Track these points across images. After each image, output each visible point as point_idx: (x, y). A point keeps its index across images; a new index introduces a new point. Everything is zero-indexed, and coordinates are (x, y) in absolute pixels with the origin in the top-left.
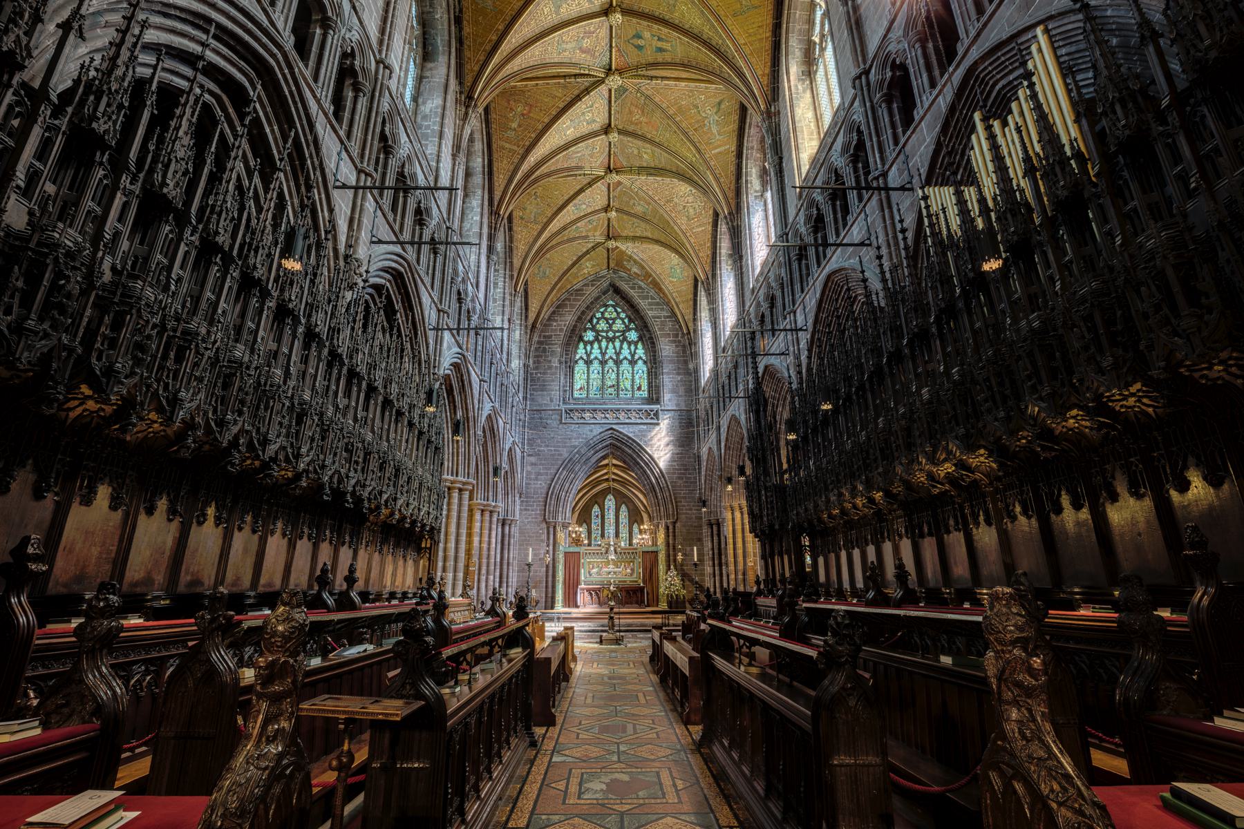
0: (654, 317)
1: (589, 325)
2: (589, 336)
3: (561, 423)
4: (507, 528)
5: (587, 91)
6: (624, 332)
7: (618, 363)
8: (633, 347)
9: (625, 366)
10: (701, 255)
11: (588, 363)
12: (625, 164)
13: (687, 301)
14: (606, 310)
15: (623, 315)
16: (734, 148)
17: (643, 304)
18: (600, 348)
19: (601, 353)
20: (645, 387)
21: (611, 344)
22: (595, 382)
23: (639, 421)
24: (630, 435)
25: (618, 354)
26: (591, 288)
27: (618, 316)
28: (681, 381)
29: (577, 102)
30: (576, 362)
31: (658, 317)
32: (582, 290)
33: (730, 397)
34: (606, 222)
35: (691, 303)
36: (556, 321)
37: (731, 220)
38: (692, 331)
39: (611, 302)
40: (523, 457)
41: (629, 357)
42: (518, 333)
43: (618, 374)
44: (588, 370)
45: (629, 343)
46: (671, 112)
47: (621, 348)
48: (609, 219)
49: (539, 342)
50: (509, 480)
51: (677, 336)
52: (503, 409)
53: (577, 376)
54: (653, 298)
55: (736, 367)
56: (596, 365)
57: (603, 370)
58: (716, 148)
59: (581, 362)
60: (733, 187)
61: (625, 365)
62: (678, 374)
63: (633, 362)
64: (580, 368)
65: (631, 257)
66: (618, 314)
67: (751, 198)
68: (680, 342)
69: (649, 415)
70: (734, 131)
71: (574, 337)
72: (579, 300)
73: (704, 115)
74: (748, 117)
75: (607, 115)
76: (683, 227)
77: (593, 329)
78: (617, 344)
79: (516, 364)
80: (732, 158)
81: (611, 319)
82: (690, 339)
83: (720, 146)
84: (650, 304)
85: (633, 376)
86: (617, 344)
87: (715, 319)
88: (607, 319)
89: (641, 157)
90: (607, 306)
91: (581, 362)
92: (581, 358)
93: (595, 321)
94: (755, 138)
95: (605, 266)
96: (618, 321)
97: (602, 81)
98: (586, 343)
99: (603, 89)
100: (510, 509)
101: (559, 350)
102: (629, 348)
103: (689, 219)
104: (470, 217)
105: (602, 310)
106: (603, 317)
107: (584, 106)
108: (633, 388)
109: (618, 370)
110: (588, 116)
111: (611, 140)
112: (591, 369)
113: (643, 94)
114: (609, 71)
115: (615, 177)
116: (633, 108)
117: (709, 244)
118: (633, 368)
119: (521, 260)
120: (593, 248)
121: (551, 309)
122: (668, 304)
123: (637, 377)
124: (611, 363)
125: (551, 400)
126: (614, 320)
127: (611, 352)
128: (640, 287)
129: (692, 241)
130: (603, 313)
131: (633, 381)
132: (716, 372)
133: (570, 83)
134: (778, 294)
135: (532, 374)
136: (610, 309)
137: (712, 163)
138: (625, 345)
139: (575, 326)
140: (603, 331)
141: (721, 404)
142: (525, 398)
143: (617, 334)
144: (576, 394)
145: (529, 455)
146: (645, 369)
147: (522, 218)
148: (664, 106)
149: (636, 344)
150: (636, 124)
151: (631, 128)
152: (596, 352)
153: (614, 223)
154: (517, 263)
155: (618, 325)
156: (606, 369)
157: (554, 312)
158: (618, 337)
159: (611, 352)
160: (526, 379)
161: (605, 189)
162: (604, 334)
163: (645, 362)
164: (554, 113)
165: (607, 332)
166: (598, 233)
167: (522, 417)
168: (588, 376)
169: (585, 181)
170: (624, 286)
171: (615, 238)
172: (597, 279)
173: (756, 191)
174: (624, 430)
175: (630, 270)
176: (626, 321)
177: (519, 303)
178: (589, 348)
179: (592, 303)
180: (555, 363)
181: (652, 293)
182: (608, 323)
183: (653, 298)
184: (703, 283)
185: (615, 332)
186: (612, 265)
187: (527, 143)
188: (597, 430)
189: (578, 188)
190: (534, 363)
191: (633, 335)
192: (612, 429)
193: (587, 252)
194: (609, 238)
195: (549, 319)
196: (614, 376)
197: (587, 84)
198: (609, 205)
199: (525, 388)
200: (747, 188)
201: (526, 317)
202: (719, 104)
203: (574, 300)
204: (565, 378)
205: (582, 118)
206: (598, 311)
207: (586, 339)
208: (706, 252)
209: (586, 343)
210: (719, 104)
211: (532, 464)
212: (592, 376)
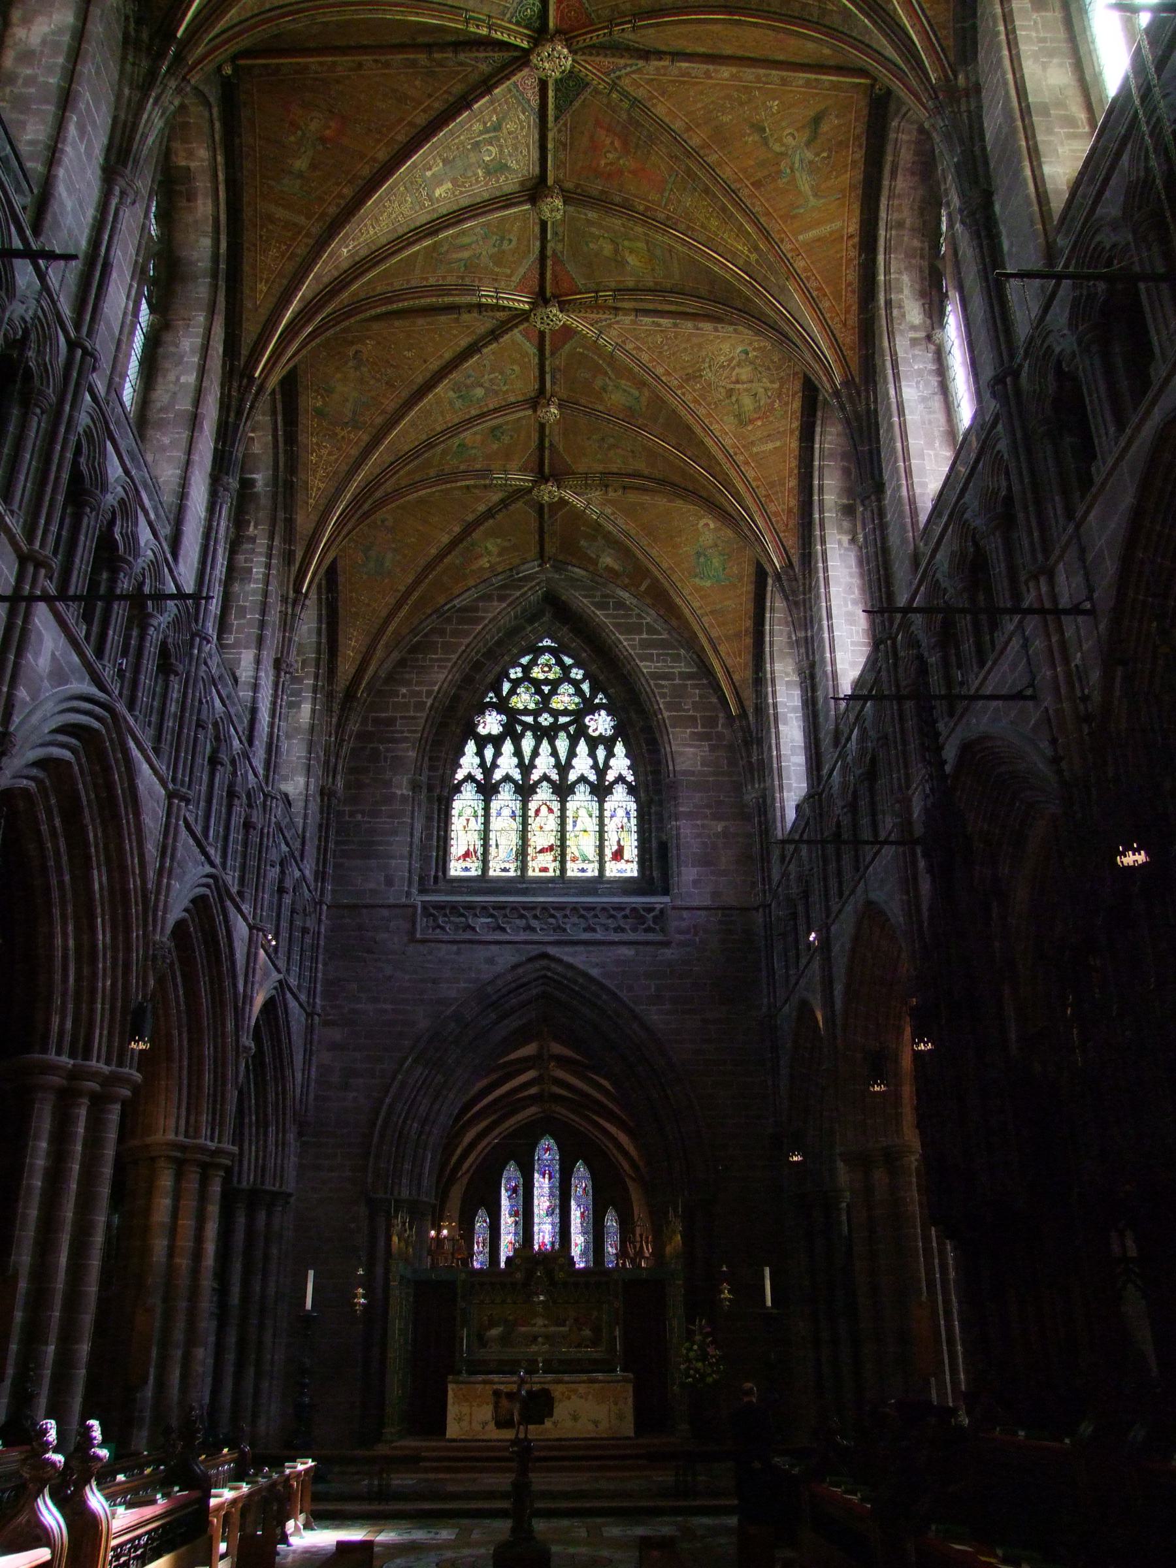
0: (656, 676)
1: (491, 697)
3: (413, 940)
4: (262, 1217)
5: (486, 86)
6: (578, 716)
7: (563, 790)
8: (601, 753)
9: (581, 800)
10: (772, 508)
11: (488, 790)
12: (581, 282)
13: (738, 635)
14: (533, 662)
15: (577, 674)
16: (853, 227)
17: (627, 644)
18: (518, 753)
19: (521, 765)
21: (545, 743)
23: (616, 937)
24: (594, 972)
25: (563, 768)
26: (498, 607)
27: (566, 678)
28: (725, 834)
29: (459, 113)
30: (457, 789)
31: (665, 676)
32: (476, 609)
33: (951, 699)
34: (535, 436)
35: (749, 641)
36: (408, 683)
37: (850, 397)
38: (750, 711)
39: (547, 642)
40: (310, 1029)
41: (592, 777)
42: (306, 708)
43: (563, 818)
44: (487, 809)
45: (593, 743)
46: (695, 141)
47: (572, 754)
48: (542, 427)
49: (362, 736)
50: (271, 1089)
51: (711, 722)
52: (249, 893)
53: (457, 824)
54: (651, 630)
55: (871, 776)
56: (506, 799)
57: (525, 808)
58: (810, 227)
59: (469, 791)
60: (853, 320)
61: (581, 800)
62: (717, 817)
63: (601, 791)
64: (466, 803)
65: (597, 527)
66: (566, 669)
67: (902, 344)
68: (720, 736)
69: (642, 920)
70: (852, 187)
72: (466, 634)
73: (777, 148)
74: (889, 148)
75: (535, 154)
76: (728, 442)
77: (502, 706)
79: (295, 785)
80: (849, 251)
81: (547, 682)
82: (747, 730)
83: (818, 223)
84: (645, 644)
85: (601, 824)
86: (562, 744)
87: (812, 666)
88: (537, 683)
89: (622, 263)
90: (538, 652)
91: (469, 791)
92: (470, 778)
93: (506, 687)
94: (906, 202)
95: (534, 551)
96: (566, 688)
97: (522, 59)
99: (525, 80)
100: (271, 1164)
101: (412, 754)
102: (592, 754)
103: (742, 421)
104: (171, 377)
105: (525, 660)
106: (527, 677)
107: (478, 127)
108: (601, 854)
109: (563, 809)
110: (490, 154)
111: (547, 214)
112: (495, 805)
113: (625, 94)
114: (540, 33)
115: (557, 317)
116: (601, 134)
117: (793, 483)
118: (601, 802)
119: (314, 517)
120: (505, 503)
121: (396, 656)
122: (690, 642)
123: (611, 826)
124: (544, 793)
125: (389, 882)
127: (544, 764)
128: (620, 605)
129: (751, 474)
131: (601, 833)
132: (815, 798)
133: (440, 64)
134: (994, 545)
135: (340, 814)
136: (546, 658)
137: (800, 264)
138: (582, 748)
139: (456, 699)
140: (526, 712)
141: (833, 883)
142: (320, 875)
143: (563, 720)
144: (456, 869)
145: (326, 1023)
146: (633, 806)
147: (320, 413)
148: (677, 125)
149: (609, 743)
150: (610, 175)
151: (596, 187)
152: (507, 764)
153: (555, 437)
154: (304, 522)
155: (565, 699)
156: (533, 806)
157: (402, 663)
158: (565, 727)
159: (544, 764)
160: (324, 827)
161: (531, 349)
162: (529, 719)
163: (632, 790)
164: (402, 138)
165: (536, 713)
166: (514, 465)
167: (310, 923)
168: (486, 823)
169: (483, 324)
170: (582, 602)
171: (558, 476)
172: (513, 583)
173: (914, 328)
174: (577, 958)
175: (595, 562)
176: (585, 687)
177: (307, 626)
178: (489, 752)
179: (499, 643)
180: (402, 788)
181: (650, 617)
182: (539, 691)
183: (651, 630)
184: (778, 577)
185: (555, 714)
186: (550, 550)
187: (332, 210)
188: (507, 958)
189: (464, 342)
190: (347, 786)
191: (601, 724)
192: (545, 956)
193: (490, 513)
194: (542, 477)
195: (390, 678)
196: (552, 823)
197: (484, 67)
198: (542, 391)
199: (322, 851)
200: (890, 317)
201: (332, 672)
202: (817, 120)
203: (456, 633)
204: (427, 827)
205: (473, 157)
207: (482, 730)
208: (785, 501)
210: (817, 120)
211: (333, 1047)
212: (495, 824)
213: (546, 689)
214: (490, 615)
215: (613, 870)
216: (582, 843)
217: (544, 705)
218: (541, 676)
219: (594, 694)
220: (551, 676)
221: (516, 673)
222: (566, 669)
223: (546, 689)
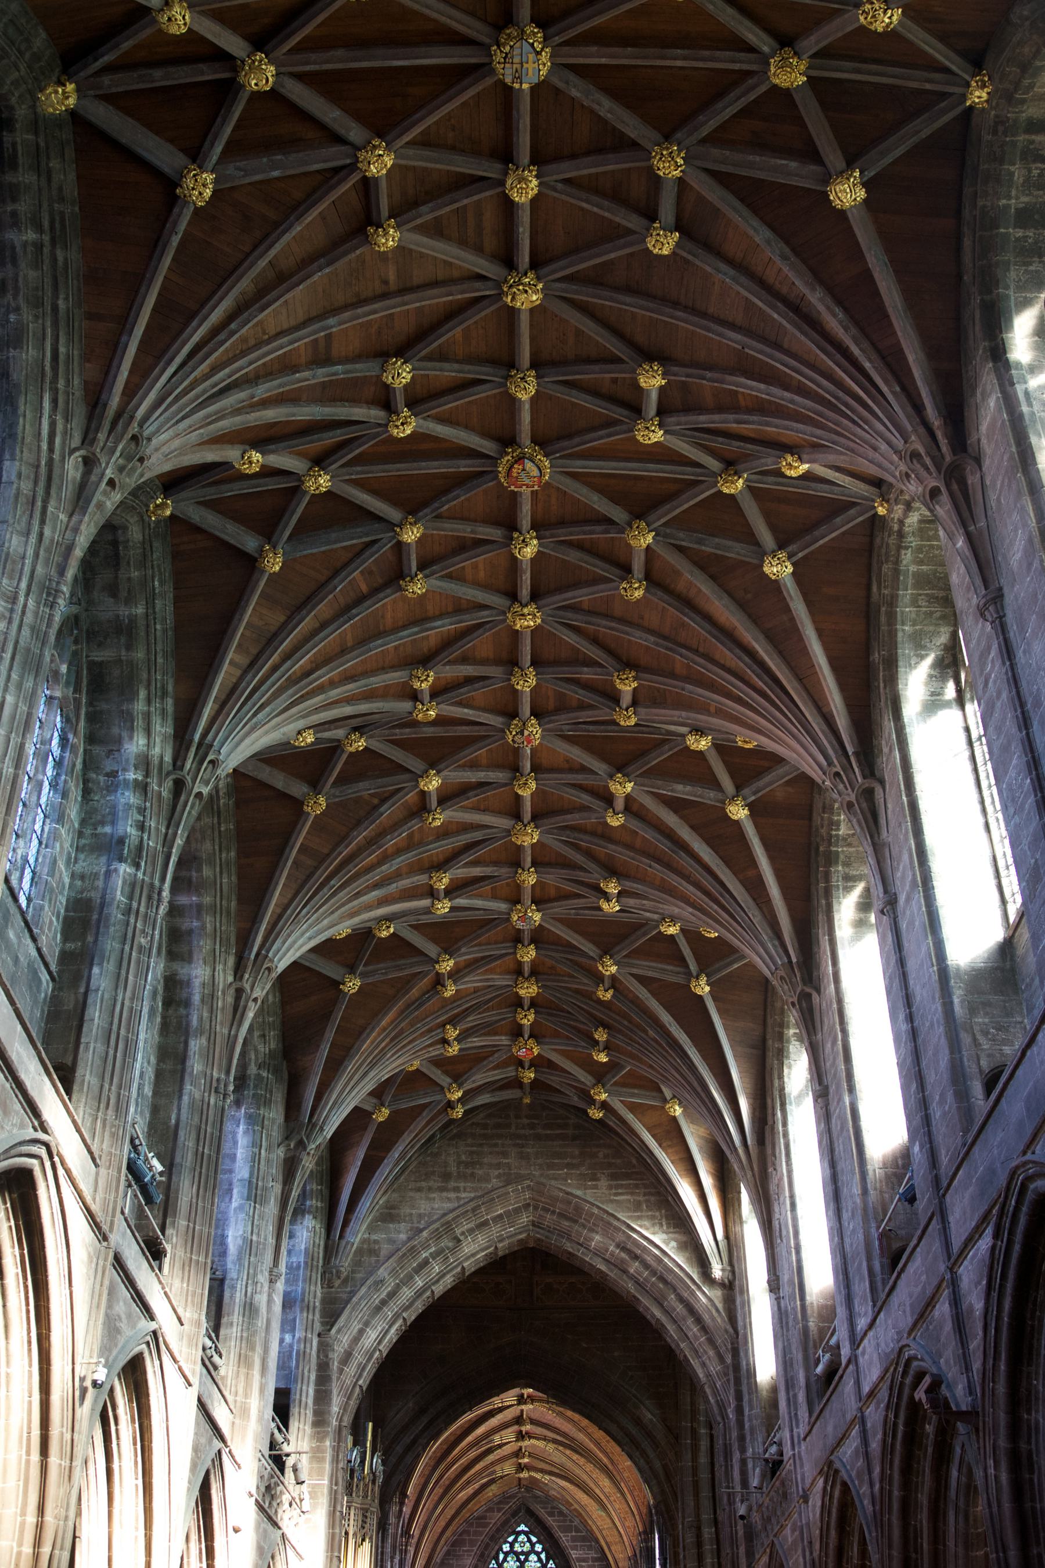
14: (515, 1540)
15: (538, 1548)
27: (532, 1551)
39: (522, 1527)
66: (533, 1545)
72: (481, 1533)
81: (522, 1553)
88: (517, 1554)
90: (519, 1533)
93: (501, 1556)
96: (533, 1557)
105: (510, 1539)
106: (512, 1550)
126: (527, 1554)
130: (512, 1545)
136: (522, 1538)
176: (543, 1556)
179: (498, 1530)
182: (518, 1560)
206: (506, 1542)
213: (522, 1558)
214: (493, 1521)
218: (520, 1550)
219: (547, 1562)
220: (525, 1549)
222: (533, 1545)
223: (522, 1558)
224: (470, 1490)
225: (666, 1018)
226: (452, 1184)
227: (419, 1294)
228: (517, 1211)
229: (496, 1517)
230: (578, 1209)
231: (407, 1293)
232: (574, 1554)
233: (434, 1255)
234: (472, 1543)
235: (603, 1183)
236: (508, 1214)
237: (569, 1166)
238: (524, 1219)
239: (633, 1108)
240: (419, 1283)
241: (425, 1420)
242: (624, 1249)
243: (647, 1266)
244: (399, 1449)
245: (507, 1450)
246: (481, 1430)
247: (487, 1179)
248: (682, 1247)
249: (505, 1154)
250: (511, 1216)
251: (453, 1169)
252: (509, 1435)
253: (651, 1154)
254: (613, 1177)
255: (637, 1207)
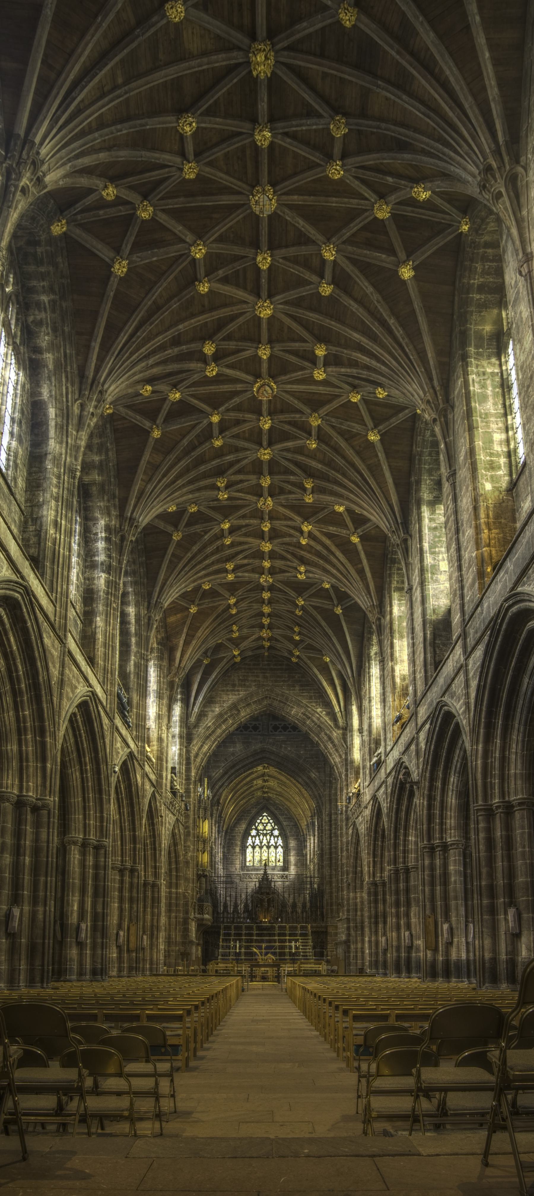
2: (254, 832)
7: (268, 847)
9: (272, 849)
11: (254, 847)
20: (282, 860)
22: (257, 858)
25: (268, 843)
45: (274, 837)
51: (297, 836)
56: (257, 849)
61: (272, 849)
63: (276, 847)
64: (249, 850)
71: (246, 834)
77: (256, 829)
78: (268, 837)
86: (268, 837)
98: (252, 837)
124: (265, 848)
127: (265, 842)
144: (248, 864)
149: (277, 837)
159: (265, 842)
191: (276, 833)
196: (266, 854)
209: (252, 837)
215: (278, 864)
216: (272, 859)
217: (265, 829)
221: (259, 821)
224: (244, 801)
225: (323, 623)
226: (236, 688)
227: (224, 731)
228: (262, 699)
229: (254, 811)
230: (287, 699)
231: (219, 731)
232: (285, 823)
233: (229, 717)
234: (246, 819)
235: (297, 688)
236: (259, 700)
237: (284, 681)
238: (265, 702)
239: (310, 658)
240: (224, 727)
241: (226, 777)
242: (304, 714)
243: (313, 722)
244: (217, 787)
245: (259, 786)
246: (248, 779)
247: (250, 686)
248: (328, 714)
249: (257, 676)
250: (259, 702)
251: (237, 682)
252: (260, 782)
253: (316, 677)
254: (301, 686)
255: (311, 698)
